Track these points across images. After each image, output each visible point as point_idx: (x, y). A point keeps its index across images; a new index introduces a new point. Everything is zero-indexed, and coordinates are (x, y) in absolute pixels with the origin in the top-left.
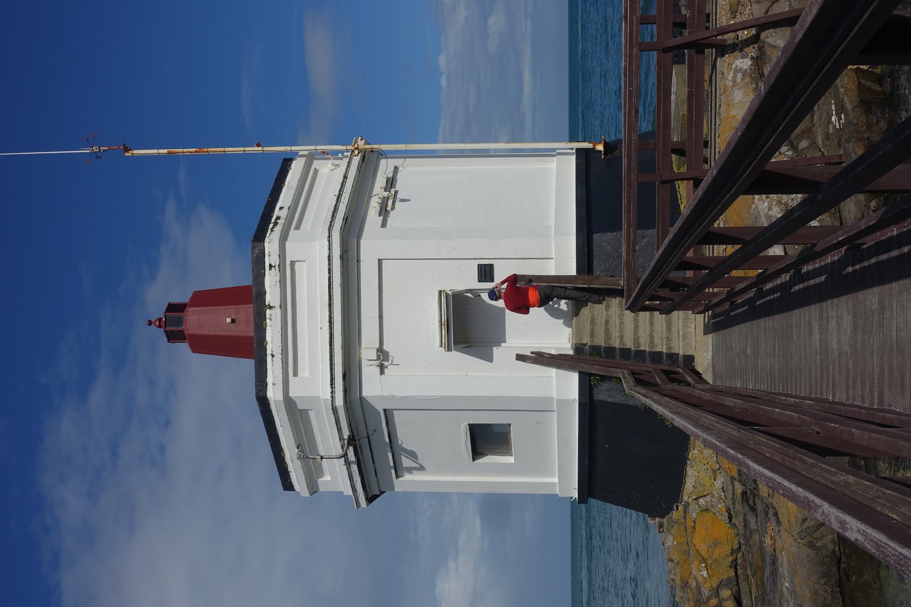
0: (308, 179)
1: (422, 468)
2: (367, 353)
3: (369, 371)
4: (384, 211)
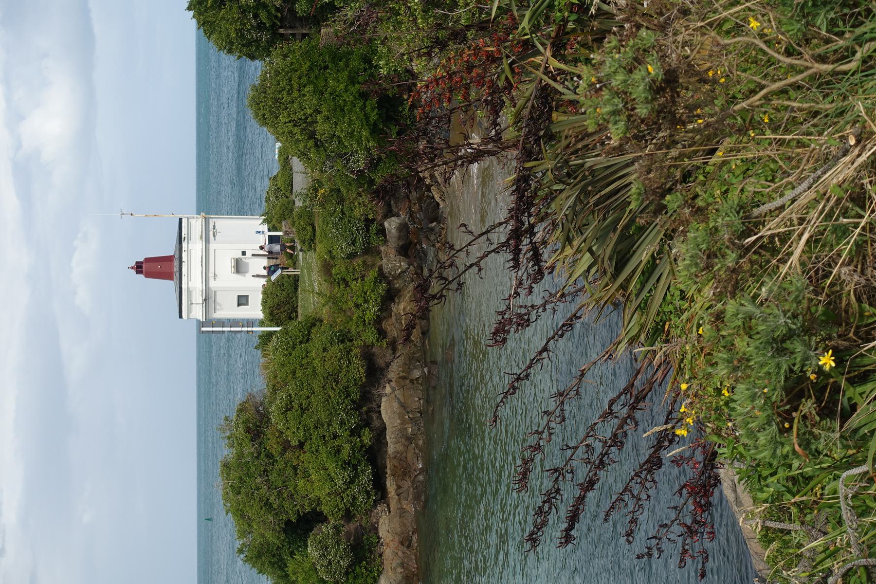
0: (189, 225)
1: (222, 309)
2: (211, 275)
3: (211, 280)
4: (214, 236)
